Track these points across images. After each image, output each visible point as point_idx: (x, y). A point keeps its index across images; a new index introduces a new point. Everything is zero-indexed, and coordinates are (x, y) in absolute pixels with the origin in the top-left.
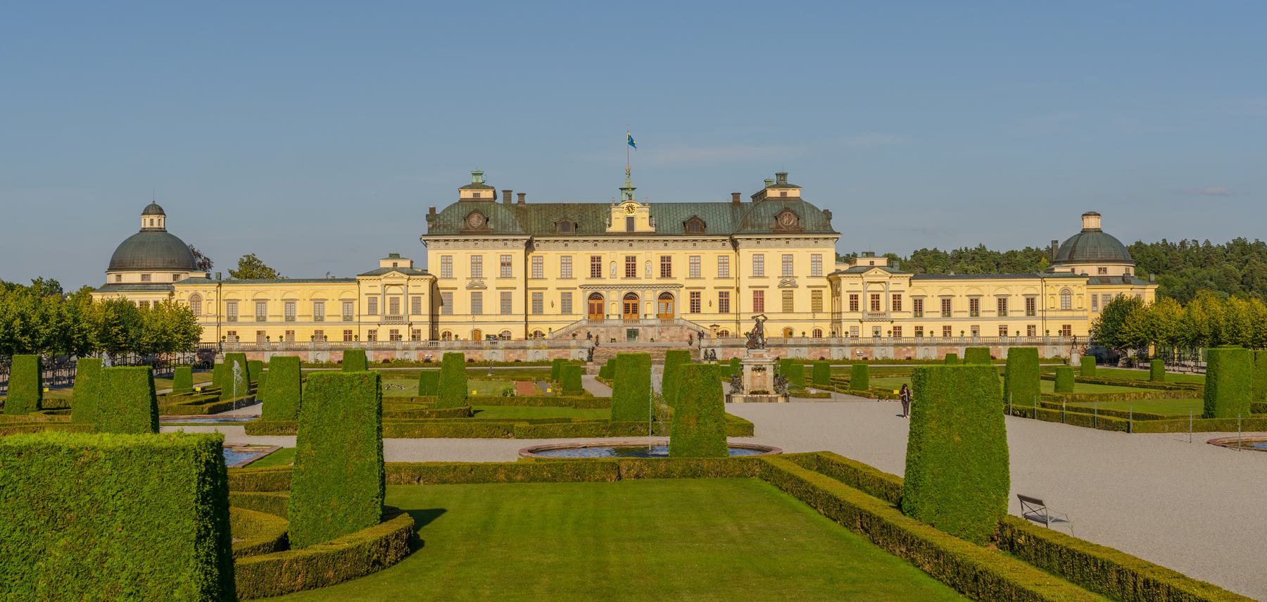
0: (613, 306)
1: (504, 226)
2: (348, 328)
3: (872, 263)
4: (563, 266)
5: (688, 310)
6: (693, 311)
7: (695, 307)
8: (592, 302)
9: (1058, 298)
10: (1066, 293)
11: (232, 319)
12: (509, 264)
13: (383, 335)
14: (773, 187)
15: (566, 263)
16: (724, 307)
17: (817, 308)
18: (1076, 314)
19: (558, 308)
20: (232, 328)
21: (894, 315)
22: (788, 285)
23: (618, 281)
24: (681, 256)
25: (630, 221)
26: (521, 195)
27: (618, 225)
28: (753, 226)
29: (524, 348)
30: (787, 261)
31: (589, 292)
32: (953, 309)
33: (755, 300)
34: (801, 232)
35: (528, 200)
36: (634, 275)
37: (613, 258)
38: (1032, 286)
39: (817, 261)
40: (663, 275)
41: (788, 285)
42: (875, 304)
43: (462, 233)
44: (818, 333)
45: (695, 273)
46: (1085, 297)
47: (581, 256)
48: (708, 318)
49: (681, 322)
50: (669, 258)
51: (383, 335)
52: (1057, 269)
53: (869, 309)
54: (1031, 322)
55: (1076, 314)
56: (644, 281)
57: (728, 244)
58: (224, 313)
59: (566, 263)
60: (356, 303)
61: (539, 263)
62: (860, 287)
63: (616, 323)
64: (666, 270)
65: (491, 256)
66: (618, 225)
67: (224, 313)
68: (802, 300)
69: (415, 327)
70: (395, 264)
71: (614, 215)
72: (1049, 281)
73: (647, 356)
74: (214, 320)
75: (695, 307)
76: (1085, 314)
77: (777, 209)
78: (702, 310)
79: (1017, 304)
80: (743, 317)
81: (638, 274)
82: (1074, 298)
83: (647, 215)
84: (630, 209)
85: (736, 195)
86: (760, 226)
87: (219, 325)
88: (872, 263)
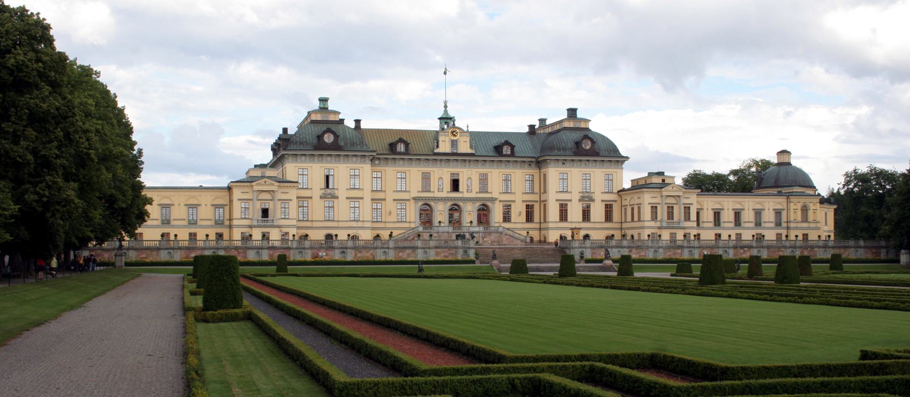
0: (441, 214)
1: (353, 144)
2: (219, 230)
3: (663, 181)
7: (507, 218)
9: (799, 212)
10: (805, 210)
13: (257, 235)
16: (529, 218)
17: (608, 217)
18: (812, 225)
23: (444, 194)
24: (496, 175)
25: (454, 143)
26: (358, 122)
27: (445, 147)
28: (559, 149)
29: (414, 248)
32: (722, 220)
33: (561, 211)
34: (596, 154)
35: (363, 126)
37: (441, 175)
38: (778, 203)
39: (609, 180)
42: (670, 215)
43: (317, 148)
46: (818, 212)
47: (414, 173)
49: (501, 229)
51: (257, 235)
54: (779, 231)
55: (812, 225)
56: (466, 195)
57: (533, 165)
63: (446, 229)
68: (598, 212)
69: (285, 230)
71: (441, 139)
72: (793, 199)
73: (563, 257)
75: (507, 218)
76: (818, 225)
77: (576, 136)
78: (513, 219)
79: (769, 217)
81: (460, 190)
82: (810, 213)
83: (468, 139)
85: (532, 127)
86: (564, 149)
88: (663, 181)
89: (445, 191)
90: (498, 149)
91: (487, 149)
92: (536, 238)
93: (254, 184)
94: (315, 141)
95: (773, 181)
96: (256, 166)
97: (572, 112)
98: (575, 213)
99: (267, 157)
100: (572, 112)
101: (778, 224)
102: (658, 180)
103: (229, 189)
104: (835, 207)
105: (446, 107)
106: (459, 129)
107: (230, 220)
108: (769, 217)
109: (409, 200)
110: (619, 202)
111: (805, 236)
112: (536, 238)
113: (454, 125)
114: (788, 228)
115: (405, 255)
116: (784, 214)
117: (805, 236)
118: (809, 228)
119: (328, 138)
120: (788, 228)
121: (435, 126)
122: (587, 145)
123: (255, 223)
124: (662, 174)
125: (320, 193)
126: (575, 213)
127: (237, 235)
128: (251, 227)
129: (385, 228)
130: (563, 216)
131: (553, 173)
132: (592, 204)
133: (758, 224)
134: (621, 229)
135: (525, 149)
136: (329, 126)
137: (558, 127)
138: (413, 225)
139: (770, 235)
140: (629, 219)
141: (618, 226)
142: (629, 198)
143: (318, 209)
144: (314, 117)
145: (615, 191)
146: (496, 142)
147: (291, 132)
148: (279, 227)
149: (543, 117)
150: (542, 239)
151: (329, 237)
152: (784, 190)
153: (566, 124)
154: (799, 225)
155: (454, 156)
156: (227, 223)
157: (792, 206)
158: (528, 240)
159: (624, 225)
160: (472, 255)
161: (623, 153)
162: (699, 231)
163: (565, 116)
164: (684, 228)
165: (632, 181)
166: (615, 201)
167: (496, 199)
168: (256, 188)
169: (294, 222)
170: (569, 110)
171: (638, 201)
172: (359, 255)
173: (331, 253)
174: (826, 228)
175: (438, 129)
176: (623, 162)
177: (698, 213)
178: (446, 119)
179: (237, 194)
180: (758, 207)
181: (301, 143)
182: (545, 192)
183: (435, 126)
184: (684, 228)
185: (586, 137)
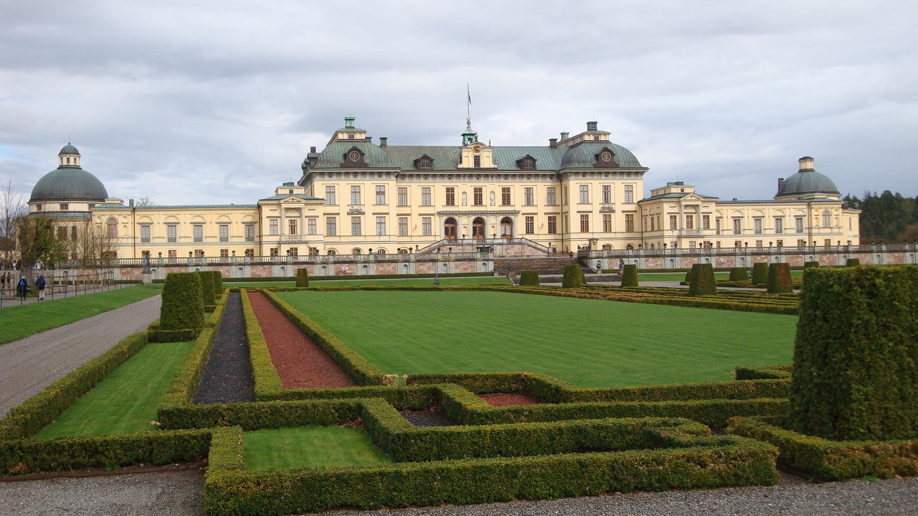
0: (465, 227)
1: (378, 161)
2: (250, 247)
3: (682, 190)
4: (425, 199)
5: (525, 232)
6: (527, 232)
7: (530, 229)
8: (447, 225)
9: (821, 218)
10: (827, 215)
11: (146, 240)
12: (384, 193)
13: (284, 250)
14: (589, 135)
15: (426, 193)
16: (552, 229)
19: (420, 231)
20: (146, 248)
21: (705, 232)
22: (607, 213)
24: (518, 188)
25: (477, 160)
27: (468, 162)
28: (579, 162)
29: (434, 261)
30: (606, 190)
31: (445, 218)
35: (389, 143)
36: (481, 203)
37: (464, 189)
38: (800, 210)
39: (629, 191)
40: (504, 204)
41: (607, 213)
42: (690, 225)
43: (342, 166)
44: (630, 247)
45: (529, 202)
47: (439, 188)
48: (541, 237)
50: (509, 189)
52: (818, 196)
53: (685, 226)
54: (800, 238)
56: (490, 209)
57: (555, 179)
58: (138, 234)
59: (426, 193)
60: (257, 226)
61: (403, 193)
62: (676, 210)
63: (470, 241)
64: (506, 200)
65: (368, 186)
66: (468, 162)
67: (138, 234)
68: (619, 222)
69: (312, 246)
70: (291, 192)
71: (464, 154)
74: (131, 241)
75: (530, 229)
77: (597, 149)
79: (790, 223)
80: (572, 236)
81: (484, 203)
84: (477, 150)
85: (553, 141)
86: (585, 162)
87: (135, 245)
88: (682, 190)
89: (469, 205)
90: (519, 163)
91: (509, 164)
92: (559, 249)
93: (282, 202)
94: (341, 160)
95: (795, 187)
96: (284, 184)
97: (592, 126)
98: (596, 223)
99: (299, 175)
100: (592, 126)
101: (800, 231)
102: (676, 190)
103: (259, 207)
104: (860, 211)
105: (468, 123)
106: (481, 144)
107: (260, 236)
108: (790, 223)
109: (433, 215)
110: (639, 211)
111: (828, 242)
112: (559, 249)
113: (476, 141)
114: (810, 235)
115: (426, 268)
116: (805, 220)
117: (828, 242)
118: (832, 234)
119: (354, 158)
120: (810, 235)
121: (459, 142)
122: (606, 158)
123: (283, 239)
124: (682, 183)
125: (348, 209)
126: (596, 223)
127: (266, 252)
128: (279, 243)
129: (411, 242)
130: (585, 227)
131: (574, 185)
132: (613, 215)
133: (737, 231)
134: (642, 238)
135: (546, 163)
136: (356, 144)
137: (579, 141)
138: (438, 239)
139: (791, 242)
140: (649, 229)
141: (639, 235)
142: (648, 208)
143: (344, 225)
144: (340, 136)
145: (635, 201)
146: (518, 156)
147: (318, 151)
148: (306, 243)
149: (566, 131)
150: (565, 250)
151: (357, 251)
152: (805, 196)
153: (587, 138)
154: (822, 231)
155: (478, 172)
156: (257, 239)
157: (814, 212)
158: (551, 250)
159: (645, 235)
160: (491, 266)
161: (643, 164)
162: (719, 239)
163: (585, 130)
164: (703, 237)
165: (652, 191)
166: (636, 211)
167: (519, 212)
168: (284, 206)
169: (321, 238)
170: (588, 123)
171: (658, 211)
172: (381, 269)
173: (353, 266)
174: (851, 233)
175: (461, 145)
176: (642, 173)
177: (718, 221)
178: (470, 137)
179: (266, 211)
180: (779, 214)
181: (328, 161)
182: (566, 204)
183: (459, 142)
184: (703, 237)
185: (606, 149)
